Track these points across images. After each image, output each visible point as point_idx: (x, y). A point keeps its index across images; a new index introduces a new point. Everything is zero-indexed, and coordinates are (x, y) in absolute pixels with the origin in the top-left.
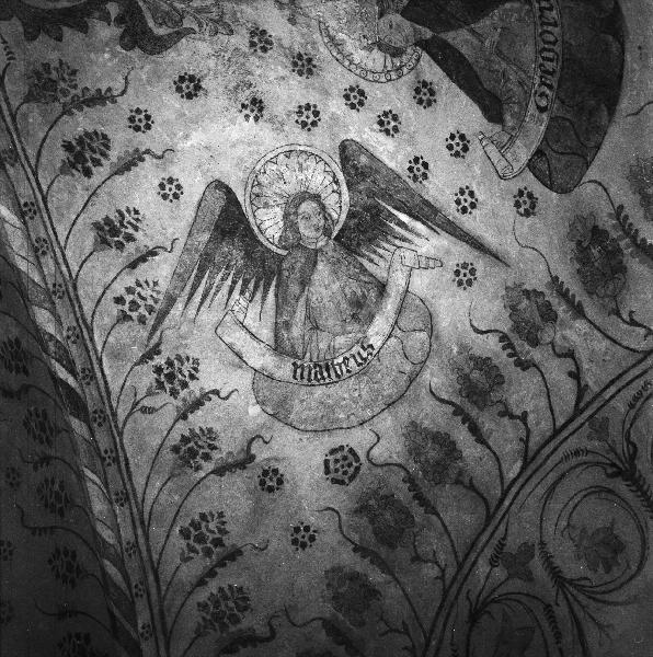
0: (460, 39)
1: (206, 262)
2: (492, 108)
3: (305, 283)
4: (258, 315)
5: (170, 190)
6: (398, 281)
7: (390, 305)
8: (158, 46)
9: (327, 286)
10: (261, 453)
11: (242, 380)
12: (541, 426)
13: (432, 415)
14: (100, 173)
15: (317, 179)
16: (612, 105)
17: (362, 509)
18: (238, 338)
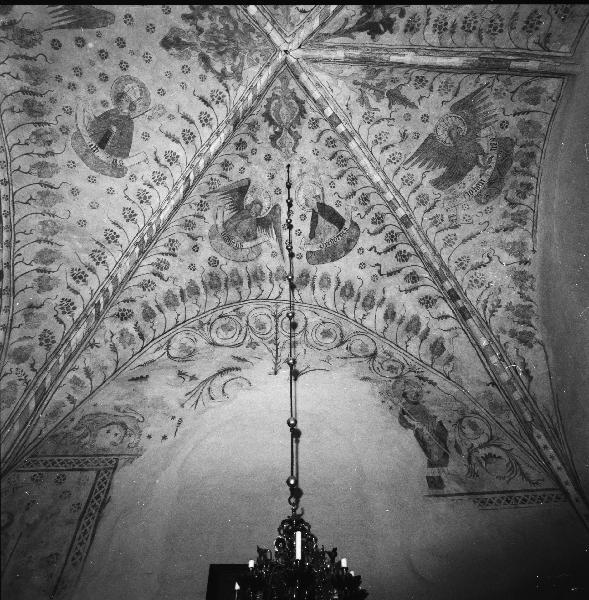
0: (320, 218)
1: (231, 192)
2: (312, 235)
3: (242, 219)
4: (228, 214)
5: (242, 171)
6: (260, 240)
7: (254, 243)
8: (274, 146)
9: (245, 225)
10: (199, 240)
11: (212, 223)
12: (265, 295)
13: (243, 272)
14: (238, 152)
15: (266, 204)
16: (332, 261)
17: (211, 275)
18: (220, 215)
